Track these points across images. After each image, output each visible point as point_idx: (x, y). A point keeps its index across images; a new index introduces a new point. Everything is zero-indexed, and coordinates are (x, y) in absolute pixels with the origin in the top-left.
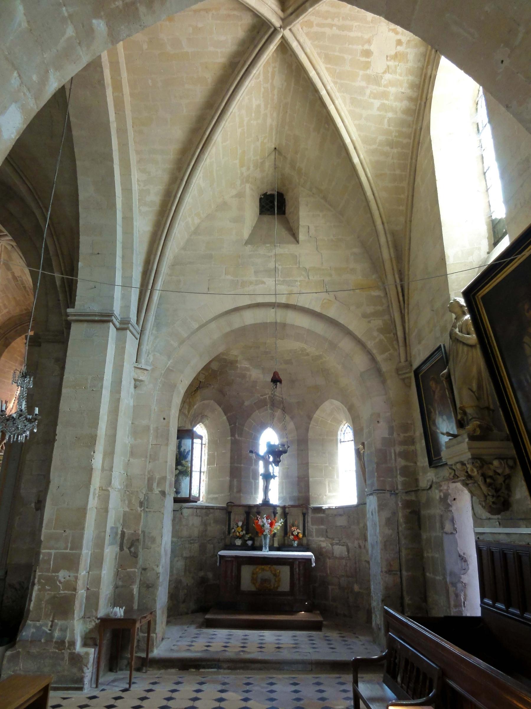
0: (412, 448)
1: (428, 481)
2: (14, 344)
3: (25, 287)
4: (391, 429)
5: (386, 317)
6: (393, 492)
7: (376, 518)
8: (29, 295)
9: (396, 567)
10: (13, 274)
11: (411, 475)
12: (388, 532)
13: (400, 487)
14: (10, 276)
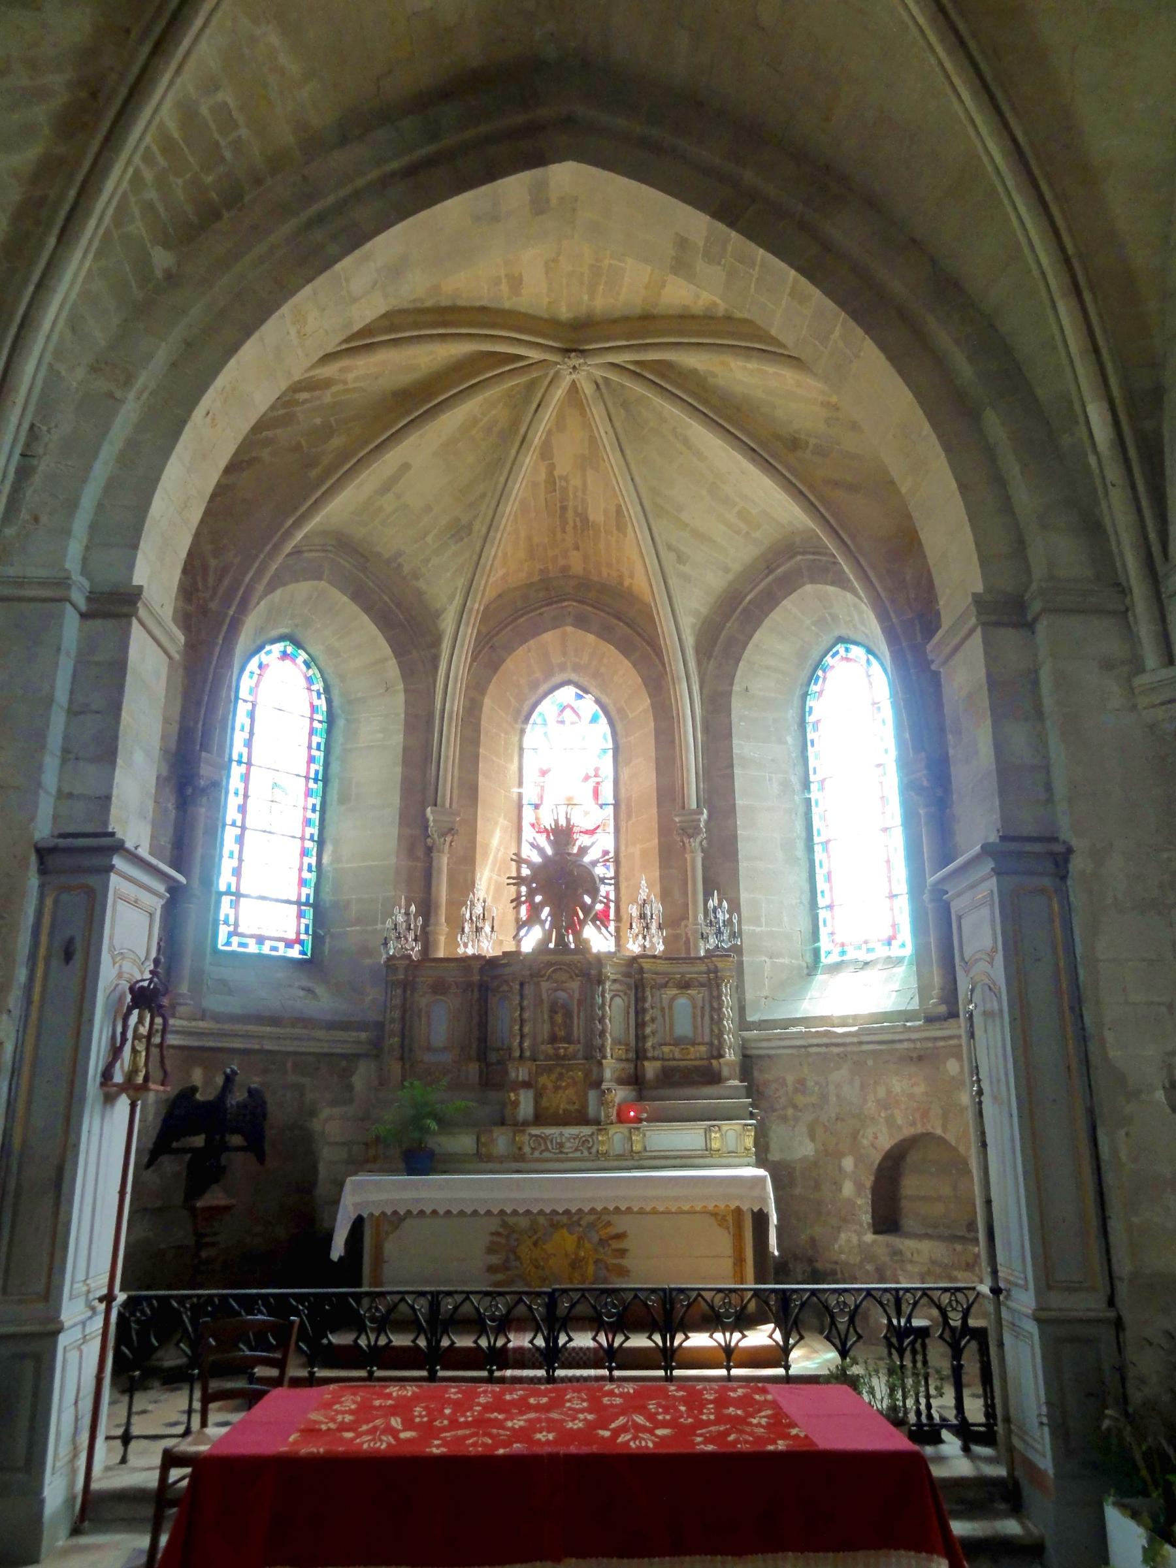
2: (509, 664)
3: (564, 509)
8: (564, 531)
10: (551, 468)
14: (543, 476)
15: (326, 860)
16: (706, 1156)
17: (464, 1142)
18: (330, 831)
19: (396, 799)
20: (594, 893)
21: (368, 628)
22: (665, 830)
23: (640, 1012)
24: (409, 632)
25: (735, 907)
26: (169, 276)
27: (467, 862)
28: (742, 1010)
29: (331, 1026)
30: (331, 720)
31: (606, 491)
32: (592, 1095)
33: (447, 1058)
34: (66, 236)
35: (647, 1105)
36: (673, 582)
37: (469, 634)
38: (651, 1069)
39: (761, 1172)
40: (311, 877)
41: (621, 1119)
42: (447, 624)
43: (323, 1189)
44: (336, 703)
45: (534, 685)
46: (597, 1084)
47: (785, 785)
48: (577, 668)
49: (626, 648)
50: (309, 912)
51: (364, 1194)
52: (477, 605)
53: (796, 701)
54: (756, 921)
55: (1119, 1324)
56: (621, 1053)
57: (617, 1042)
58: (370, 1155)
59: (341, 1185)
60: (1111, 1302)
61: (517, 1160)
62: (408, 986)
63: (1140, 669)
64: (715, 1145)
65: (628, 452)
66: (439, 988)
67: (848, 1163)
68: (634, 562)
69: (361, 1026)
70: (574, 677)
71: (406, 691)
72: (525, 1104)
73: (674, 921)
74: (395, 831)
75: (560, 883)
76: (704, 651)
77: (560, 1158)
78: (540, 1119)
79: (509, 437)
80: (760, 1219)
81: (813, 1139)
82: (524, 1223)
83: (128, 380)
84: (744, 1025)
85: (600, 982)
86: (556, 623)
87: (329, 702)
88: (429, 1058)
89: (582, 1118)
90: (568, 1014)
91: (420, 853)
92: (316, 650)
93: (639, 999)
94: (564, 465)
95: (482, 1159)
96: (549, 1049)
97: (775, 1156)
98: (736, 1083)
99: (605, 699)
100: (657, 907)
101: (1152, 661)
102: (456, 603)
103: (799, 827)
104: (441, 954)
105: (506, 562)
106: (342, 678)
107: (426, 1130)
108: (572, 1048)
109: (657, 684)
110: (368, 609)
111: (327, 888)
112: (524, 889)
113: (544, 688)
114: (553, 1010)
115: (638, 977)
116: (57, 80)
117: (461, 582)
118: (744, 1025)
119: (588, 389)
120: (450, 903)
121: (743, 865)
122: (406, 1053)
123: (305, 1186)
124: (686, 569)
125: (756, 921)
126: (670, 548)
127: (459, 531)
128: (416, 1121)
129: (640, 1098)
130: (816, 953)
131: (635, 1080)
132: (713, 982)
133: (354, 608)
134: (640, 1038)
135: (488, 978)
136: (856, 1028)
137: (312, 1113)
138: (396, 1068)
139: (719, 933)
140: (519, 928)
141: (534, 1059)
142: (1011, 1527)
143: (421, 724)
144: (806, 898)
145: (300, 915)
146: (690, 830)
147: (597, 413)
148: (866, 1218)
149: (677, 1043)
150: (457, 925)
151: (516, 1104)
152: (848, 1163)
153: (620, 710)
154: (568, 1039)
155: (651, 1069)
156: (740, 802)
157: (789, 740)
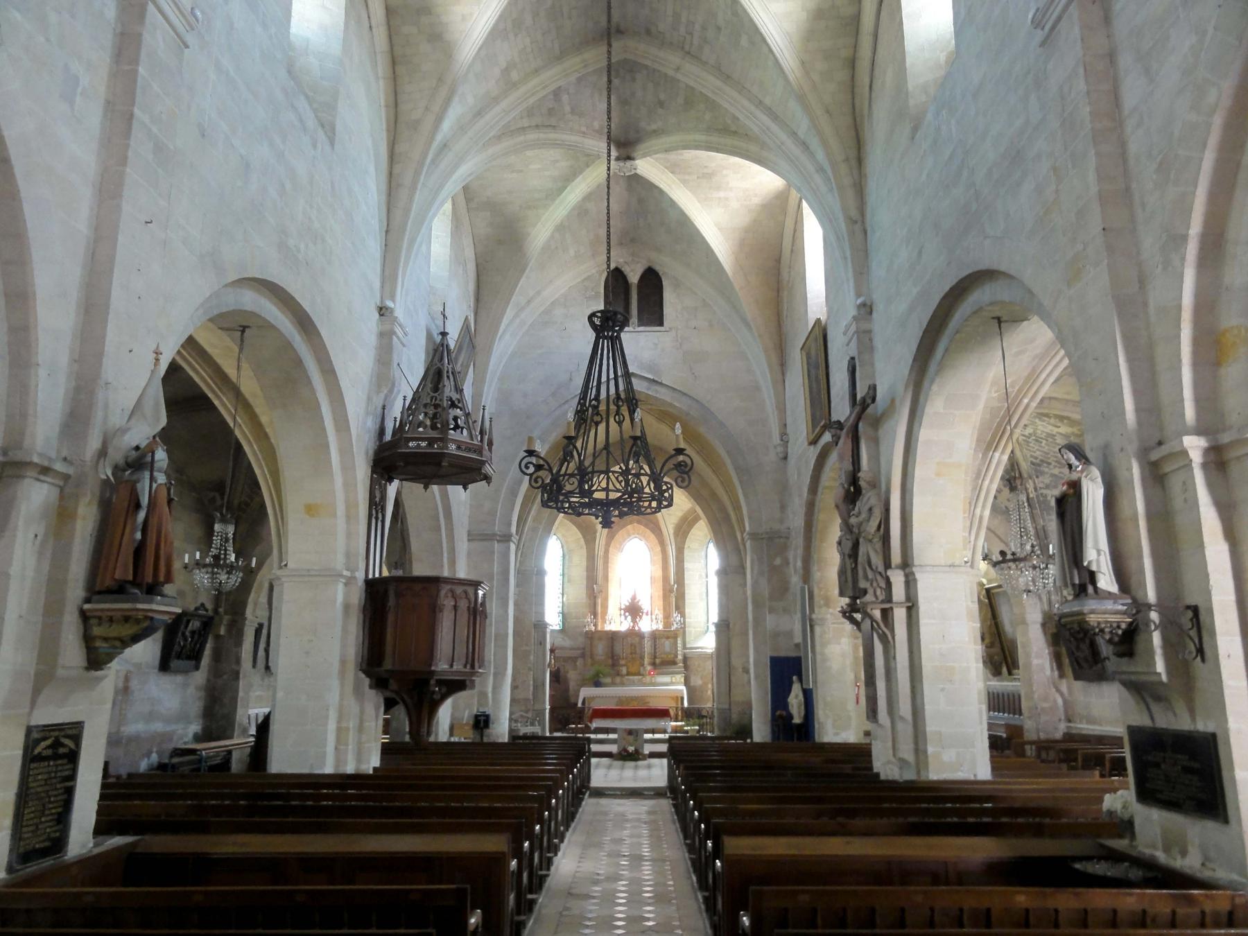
16: (672, 683)
17: (608, 680)
22: (664, 590)
25: (683, 615)
27: (606, 599)
39: (684, 688)
43: (571, 692)
49: (653, 531)
51: (586, 692)
58: (584, 683)
61: (622, 684)
69: (578, 649)
72: (624, 670)
73: (667, 616)
75: (634, 610)
76: (676, 534)
77: (633, 684)
78: (628, 674)
80: (682, 698)
84: (684, 647)
89: (639, 674)
95: (613, 684)
100: (661, 616)
109: (662, 543)
115: (655, 636)
118: (684, 647)
122: (592, 657)
123: (567, 690)
128: (597, 674)
131: (654, 664)
132: (675, 638)
135: (613, 637)
143: (591, 558)
146: (671, 591)
150: (604, 621)
155: (658, 661)
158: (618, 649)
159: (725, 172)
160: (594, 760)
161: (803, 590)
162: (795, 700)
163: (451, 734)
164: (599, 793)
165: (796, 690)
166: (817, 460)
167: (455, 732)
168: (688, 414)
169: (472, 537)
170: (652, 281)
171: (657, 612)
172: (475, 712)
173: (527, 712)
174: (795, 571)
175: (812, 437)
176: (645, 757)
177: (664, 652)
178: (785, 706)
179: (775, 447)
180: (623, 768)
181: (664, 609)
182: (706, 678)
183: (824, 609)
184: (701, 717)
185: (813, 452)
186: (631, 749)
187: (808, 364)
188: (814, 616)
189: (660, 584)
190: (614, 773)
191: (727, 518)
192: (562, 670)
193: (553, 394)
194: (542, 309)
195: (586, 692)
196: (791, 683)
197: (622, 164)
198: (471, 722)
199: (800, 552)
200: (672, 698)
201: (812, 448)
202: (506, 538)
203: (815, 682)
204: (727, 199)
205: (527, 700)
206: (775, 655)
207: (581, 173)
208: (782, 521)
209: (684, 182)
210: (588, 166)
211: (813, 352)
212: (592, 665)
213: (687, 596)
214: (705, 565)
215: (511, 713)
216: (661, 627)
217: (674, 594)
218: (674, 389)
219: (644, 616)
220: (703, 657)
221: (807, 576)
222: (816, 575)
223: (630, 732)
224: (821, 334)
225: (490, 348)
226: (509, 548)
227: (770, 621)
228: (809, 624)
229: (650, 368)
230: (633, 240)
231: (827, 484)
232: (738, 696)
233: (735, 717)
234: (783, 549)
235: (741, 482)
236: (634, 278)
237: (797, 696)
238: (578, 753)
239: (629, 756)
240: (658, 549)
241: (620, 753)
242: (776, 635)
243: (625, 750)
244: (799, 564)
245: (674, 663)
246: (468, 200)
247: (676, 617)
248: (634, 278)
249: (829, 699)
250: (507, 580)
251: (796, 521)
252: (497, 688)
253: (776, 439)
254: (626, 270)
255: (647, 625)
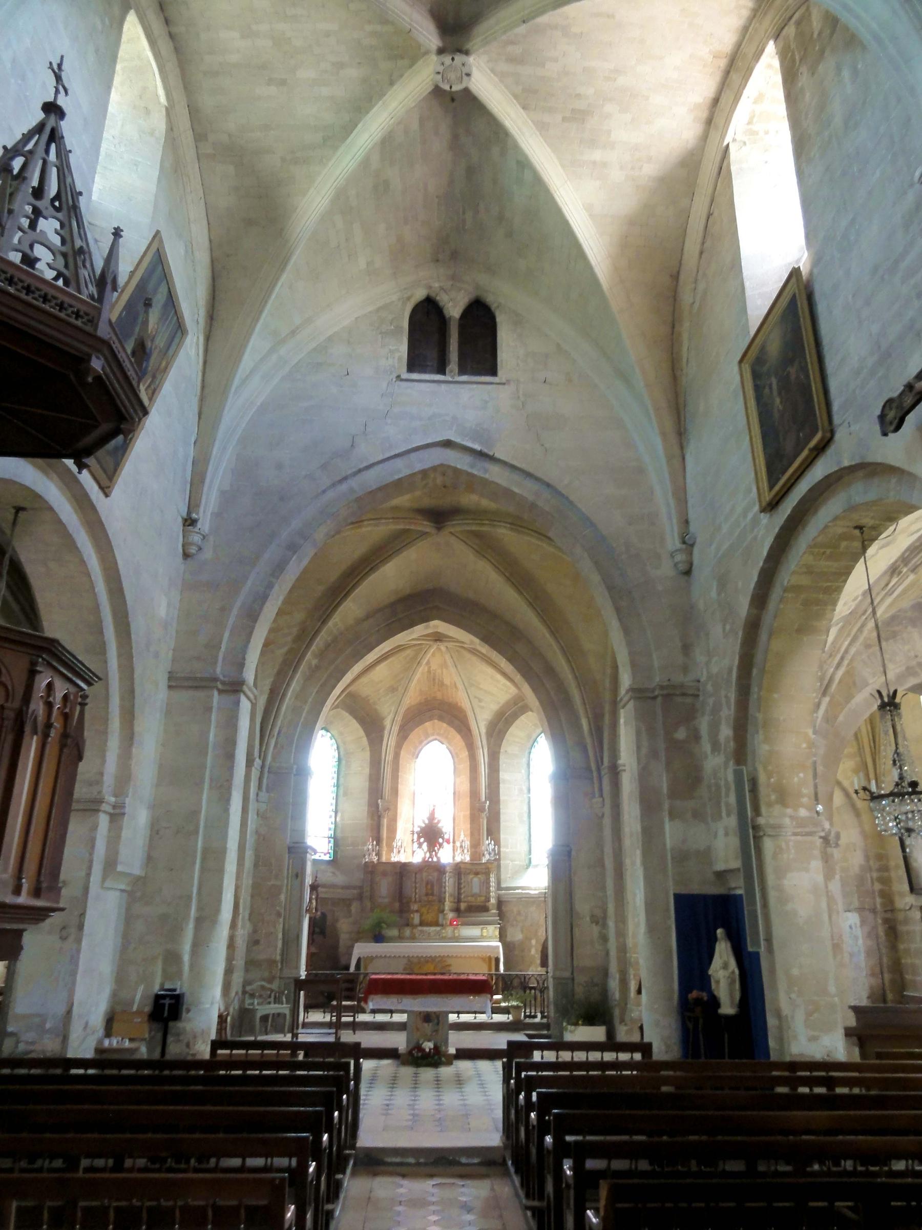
0: (886, 874)
1: (906, 904)
2: (411, 736)
3: (434, 679)
4: (867, 858)
5: (858, 759)
6: (874, 911)
7: (859, 932)
9: (878, 970)
11: (888, 898)
12: (869, 943)
13: (878, 906)
15: (338, 819)
17: (394, 932)
18: (340, 808)
19: (366, 795)
20: (443, 838)
21: (355, 725)
22: (472, 808)
23: (459, 884)
24: (372, 726)
25: (497, 843)
26: (316, 666)
27: (394, 820)
28: (499, 882)
29: (343, 888)
30: (339, 760)
31: (450, 676)
32: (441, 916)
33: (386, 900)
34: (295, 671)
35: (461, 919)
36: (477, 711)
37: (396, 729)
38: (463, 906)
39: (499, 944)
40: (333, 826)
41: (451, 924)
42: (387, 723)
43: (342, 949)
44: (342, 753)
45: (421, 742)
46: (443, 911)
47: (521, 790)
48: (438, 734)
49: (459, 731)
50: (332, 840)
51: (362, 949)
52: (399, 718)
53: (526, 754)
54: (507, 847)
55: (573, 979)
56: (452, 899)
57: (451, 895)
58: (360, 936)
59: (353, 947)
60: (572, 973)
61: (413, 938)
62: (372, 873)
63: (594, 797)
64: (485, 934)
65: (459, 667)
66: (385, 874)
67: (534, 942)
68: (462, 698)
69: (355, 888)
70: (438, 737)
71: (371, 751)
72: (416, 919)
73: (475, 845)
74: (366, 808)
75: (431, 835)
77: (429, 938)
78: (422, 924)
79: (415, 661)
80: (497, 960)
81: (522, 932)
82: (416, 960)
83: (306, 702)
84: (499, 887)
85: (444, 873)
86: (431, 719)
87: (339, 753)
88: (380, 900)
89: (437, 924)
90: (432, 886)
91: (376, 818)
92: (335, 732)
93: (459, 879)
94: (434, 666)
95: (401, 938)
96: (425, 898)
97: (509, 939)
98: (494, 911)
99: (452, 749)
100: (467, 843)
101: (597, 795)
102: (391, 716)
103: (525, 808)
104: (384, 859)
105: (412, 697)
106: (344, 743)
107: (381, 927)
108: (435, 898)
110: (356, 718)
111: (338, 831)
112: (416, 836)
113: (425, 742)
114: (427, 883)
115: (459, 870)
116: (295, 630)
117: (393, 709)
118: (499, 887)
119: (443, 648)
120: (388, 838)
121: (502, 824)
122: (372, 898)
123: (335, 947)
124: (482, 704)
125: (507, 847)
126: (475, 697)
127: (393, 689)
128: (379, 924)
129: (459, 917)
130: (530, 859)
131: (457, 910)
132: (487, 874)
133: (351, 718)
134: (459, 894)
135: (402, 870)
136: (536, 892)
137: (337, 920)
138: (368, 904)
139: (490, 854)
140: (413, 852)
141: (420, 901)
142: (545, 1032)
143: (376, 763)
144: (527, 837)
145: (329, 842)
146: (482, 810)
147: (447, 657)
148: (539, 962)
149: (472, 896)
150: (390, 849)
151: (413, 918)
152: (534, 942)
153: (456, 753)
154: (432, 894)
155: (463, 906)
156: (502, 798)
157: (523, 771)
158: (409, 885)
159: (609, 108)
160: (367, 1065)
161: (738, 775)
162: (723, 968)
163: (108, 1033)
164: (375, 1162)
165: (723, 953)
166: (778, 537)
167: (116, 1026)
168: (533, 506)
169: (175, 682)
170: (480, 321)
171: (462, 837)
172: (156, 989)
173: (271, 980)
174: (716, 747)
175: (768, 497)
176: (450, 1060)
177: (472, 893)
178: (704, 981)
179: (672, 556)
180: (415, 1085)
181: (472, 834)
182: (537, 930)
183: (777, 809)
184: (525, 987)
185: (768, 529)
186: (428, 1046)
187: (756, 376)
188: (761, 821)
189: (466, 801)
190: (402, 1097)
191: (567, 701)
192: (329, 918)
193: (324, 467)
194: (314, 345)
195: (362, 949)
196: (713, 940)
197: (447, 59)
198: (148, 1009)
199: (728, 712)
200: (483, 959)
201: (764, 518)
202: (235, 687)
203: (769, 940)
204: (604, 165)
205: (272, 962)
206: (677, 892)
207: (382, 95)
208: (685, 669)
209: (542, 127)
210: (392, 83)
211: (774, 348)
212: (372, 910)
213: (502, 818)
214: (534, 771)
215: (246, 983)
216: (467, 858)
217: (485, 814)
218: (513, 467)
219: (445, 844)
220: (528, 901)
221: (741, 751)
222: (761, 746)
223: (427, 1017)
224: (798, 302)
225: (225, 392)
226: (238, 703)
227: (671, 833)
228: (751, 836)
229: (477, 435)
230: (454, 256)
231: (795, 580)
232: (586, 957)
233: (580, 991)
234: (689, 716)
235: (618, 610)
236: (454, 309)
237: (725, 966)
238: (333, 1077)
239: (426, 1057)
240: (465, 754)
241: (410, 1053)
242: (682, 857)
243: (419, 1048)
244: (726, 732)
245: (484, 909)
246: (199, 137)
247: (488, 844)
248: (454, 309)
249: (795, 972)
250: (230, 756)
251: (718, 656)
252: (199, 945)
253: (673, 542)
254: (443, 299)
255: (446, 856)
